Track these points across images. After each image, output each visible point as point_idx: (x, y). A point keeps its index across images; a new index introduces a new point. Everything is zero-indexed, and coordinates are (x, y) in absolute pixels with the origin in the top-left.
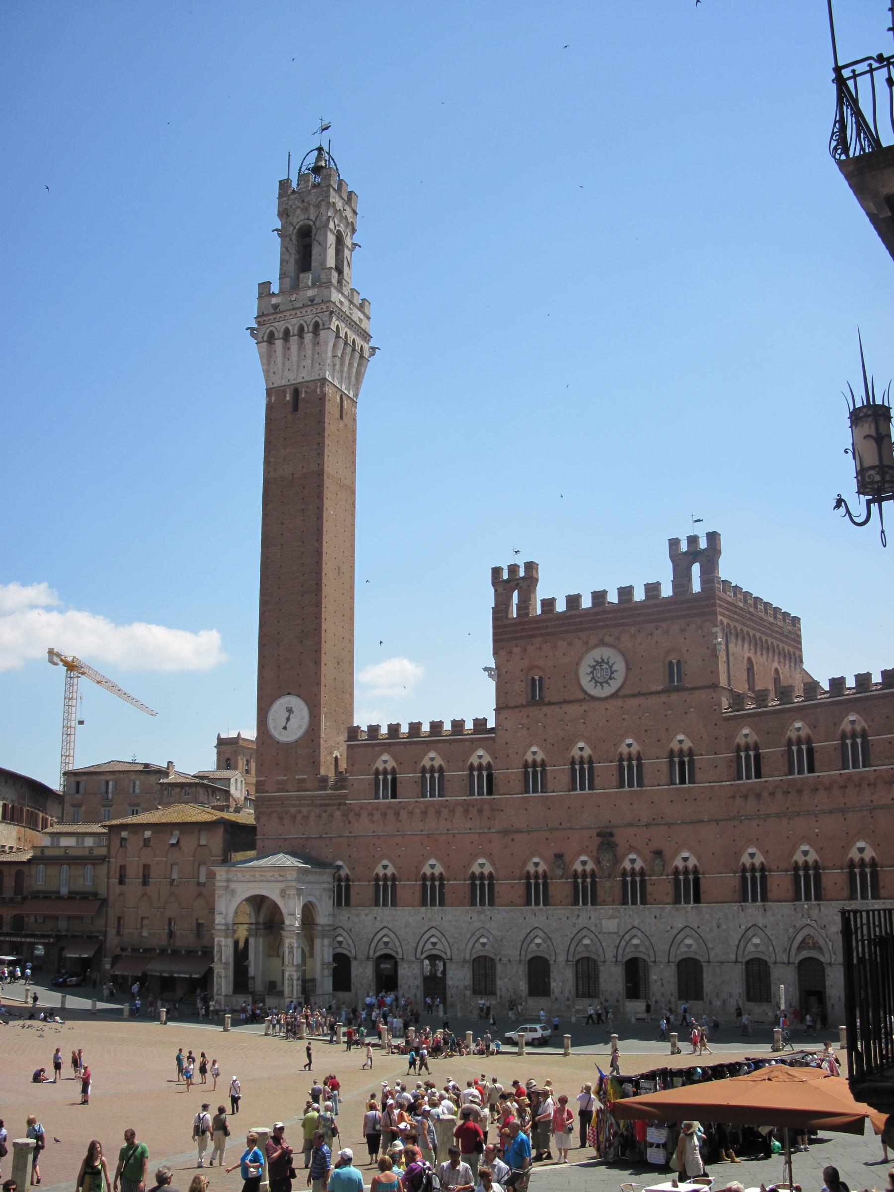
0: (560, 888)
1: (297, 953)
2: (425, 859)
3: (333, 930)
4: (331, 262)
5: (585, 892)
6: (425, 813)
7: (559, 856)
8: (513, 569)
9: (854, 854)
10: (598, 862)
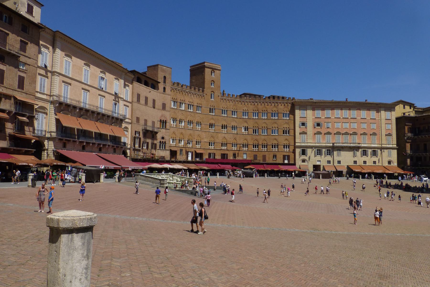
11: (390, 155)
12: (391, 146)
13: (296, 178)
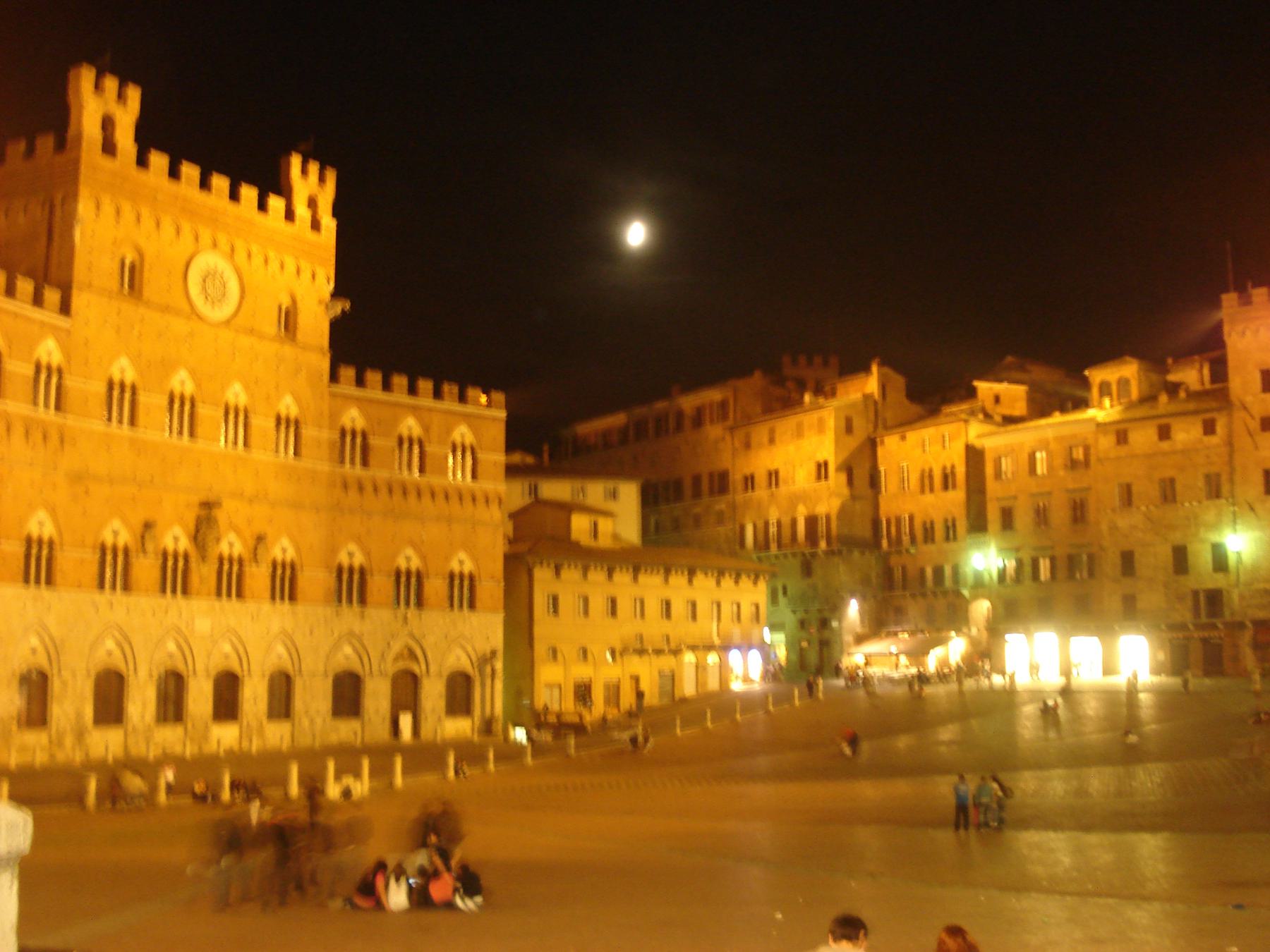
0: (147, 569)
5: (175, 577)
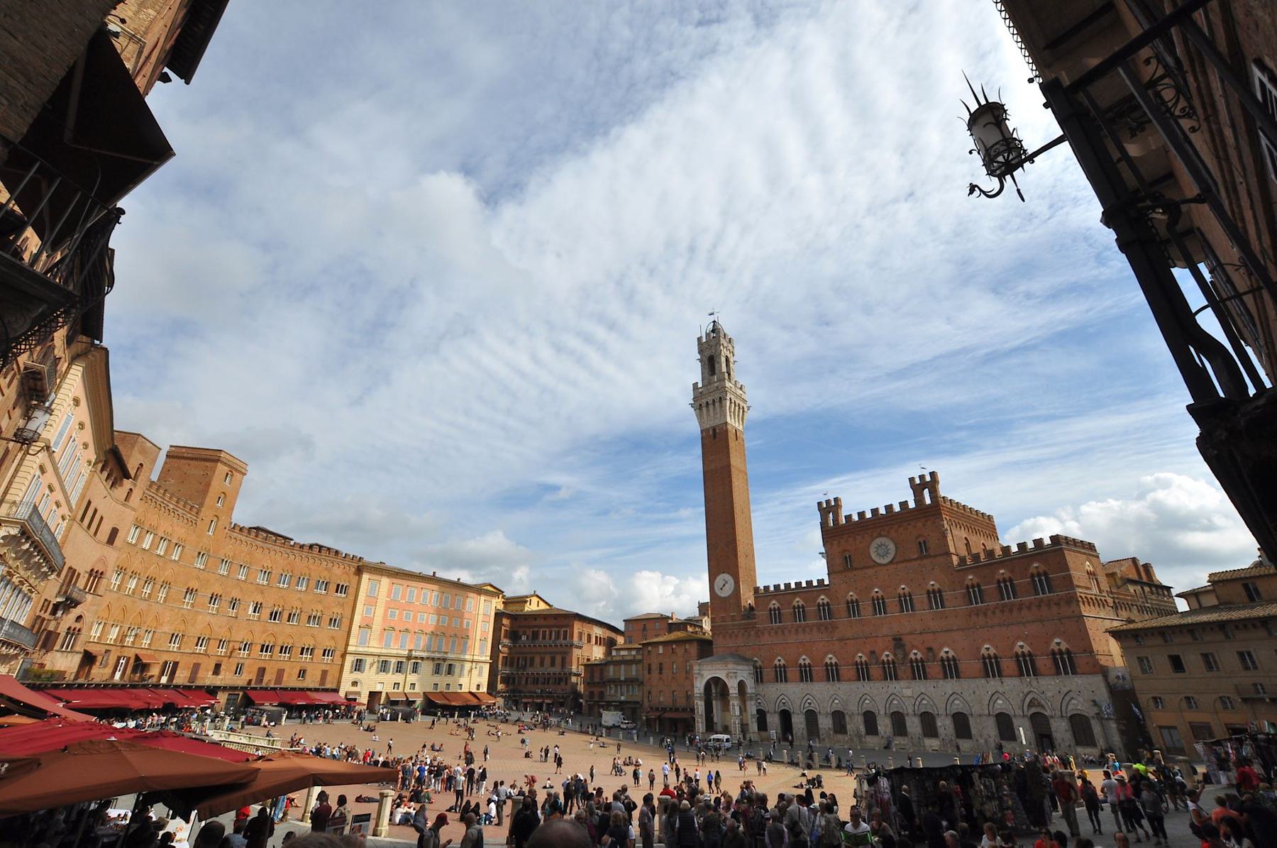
0: (875, 670)
1: (737, 709)
2: (800, 655)
3: (756, 696)
4: (724, 369)
5: (890, 672)
6: (797, 631)
7: (873, 652)
8: (828, 502)
9: (1053, 646)
10: (895, 655)
11: (480, 674)
12: (483, 659)
13: (336, 722)
